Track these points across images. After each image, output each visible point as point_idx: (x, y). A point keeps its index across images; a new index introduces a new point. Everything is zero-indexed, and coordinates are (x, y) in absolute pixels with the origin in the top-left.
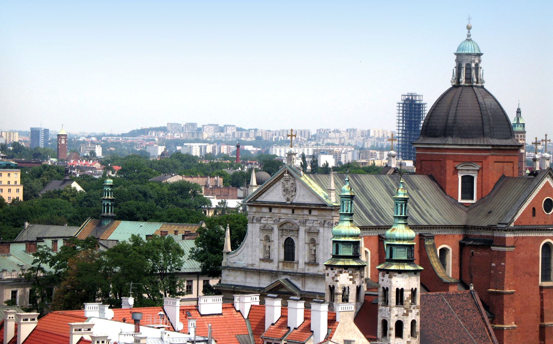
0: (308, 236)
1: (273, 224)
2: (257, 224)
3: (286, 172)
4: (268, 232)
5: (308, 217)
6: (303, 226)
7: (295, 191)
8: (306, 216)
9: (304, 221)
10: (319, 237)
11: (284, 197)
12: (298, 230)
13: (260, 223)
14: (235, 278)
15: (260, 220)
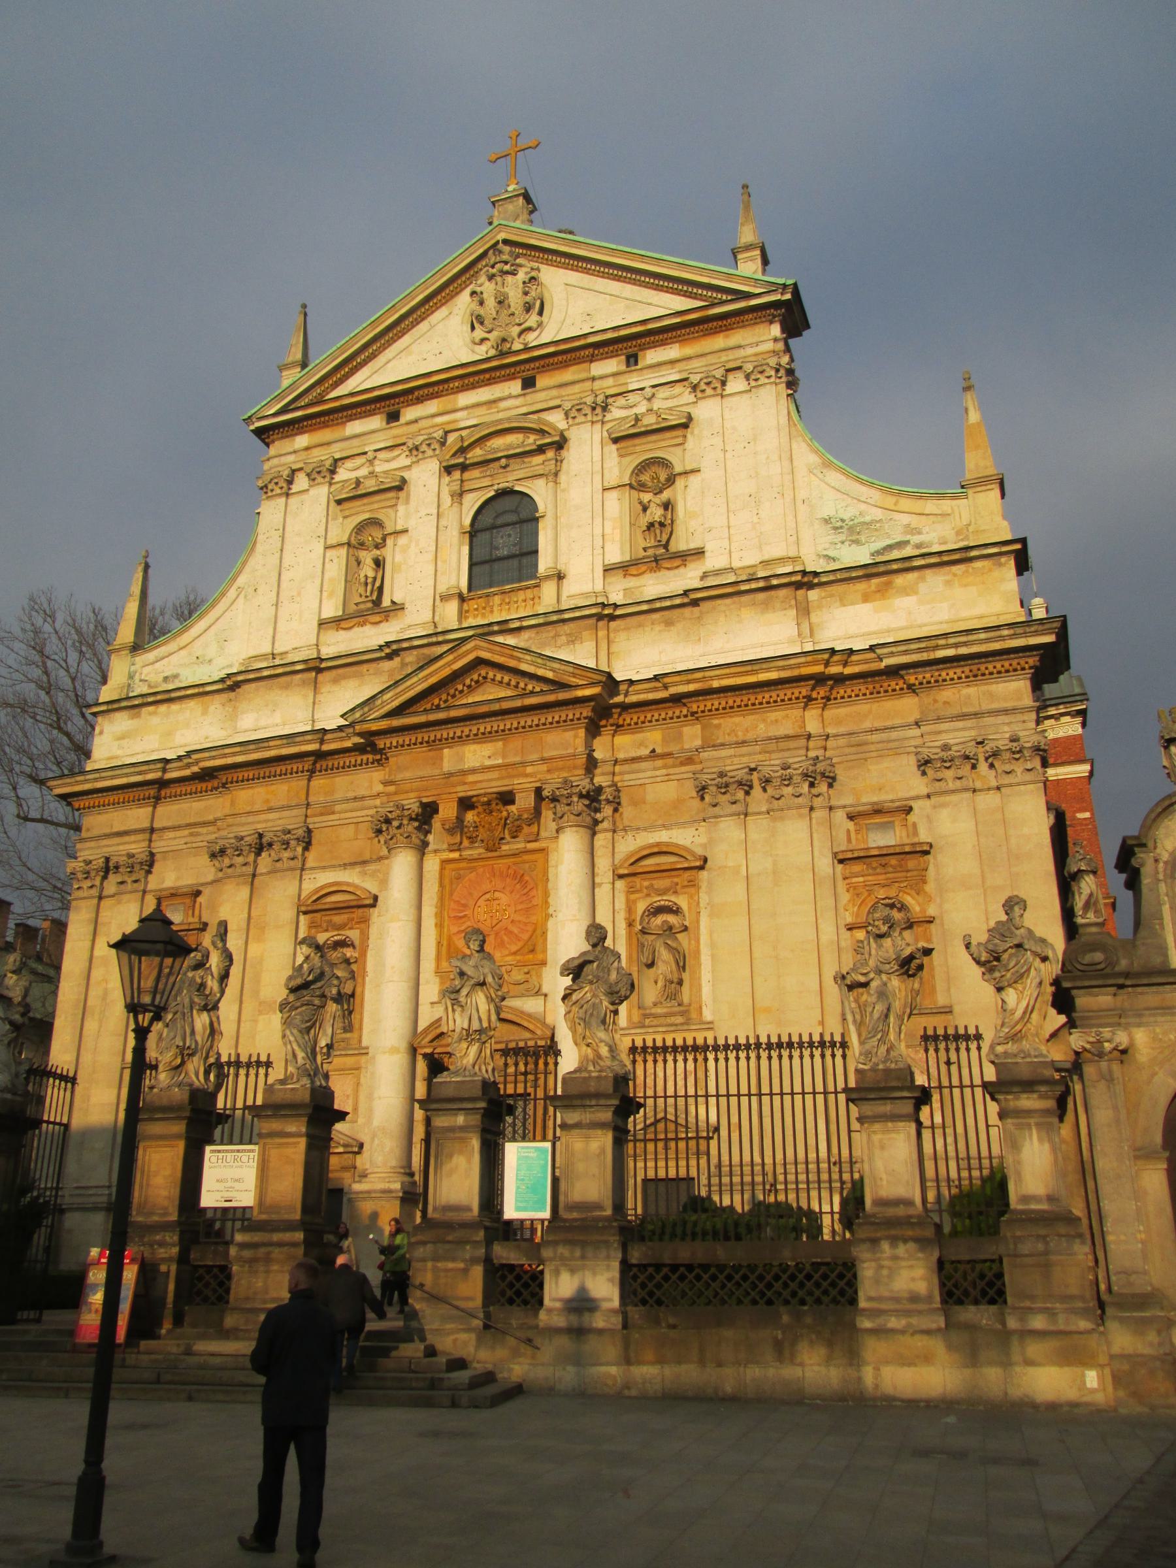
0: (621, 456)
1: (408, 467)
2: (313, 492)
3: (501, 244)
4: (376, 506)
5: (622, 379)
6: (593, 422)
7: (541, 313)
8: (610, 381)
9: (600, 399)
10: (691, 443)
11: (477, 348)
12: (560, 444)
13: (331, 484)
14: (169, 734)
15: (333, 472)
